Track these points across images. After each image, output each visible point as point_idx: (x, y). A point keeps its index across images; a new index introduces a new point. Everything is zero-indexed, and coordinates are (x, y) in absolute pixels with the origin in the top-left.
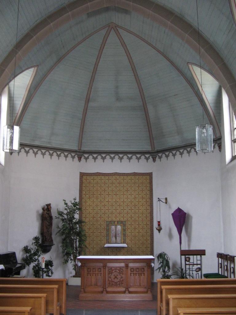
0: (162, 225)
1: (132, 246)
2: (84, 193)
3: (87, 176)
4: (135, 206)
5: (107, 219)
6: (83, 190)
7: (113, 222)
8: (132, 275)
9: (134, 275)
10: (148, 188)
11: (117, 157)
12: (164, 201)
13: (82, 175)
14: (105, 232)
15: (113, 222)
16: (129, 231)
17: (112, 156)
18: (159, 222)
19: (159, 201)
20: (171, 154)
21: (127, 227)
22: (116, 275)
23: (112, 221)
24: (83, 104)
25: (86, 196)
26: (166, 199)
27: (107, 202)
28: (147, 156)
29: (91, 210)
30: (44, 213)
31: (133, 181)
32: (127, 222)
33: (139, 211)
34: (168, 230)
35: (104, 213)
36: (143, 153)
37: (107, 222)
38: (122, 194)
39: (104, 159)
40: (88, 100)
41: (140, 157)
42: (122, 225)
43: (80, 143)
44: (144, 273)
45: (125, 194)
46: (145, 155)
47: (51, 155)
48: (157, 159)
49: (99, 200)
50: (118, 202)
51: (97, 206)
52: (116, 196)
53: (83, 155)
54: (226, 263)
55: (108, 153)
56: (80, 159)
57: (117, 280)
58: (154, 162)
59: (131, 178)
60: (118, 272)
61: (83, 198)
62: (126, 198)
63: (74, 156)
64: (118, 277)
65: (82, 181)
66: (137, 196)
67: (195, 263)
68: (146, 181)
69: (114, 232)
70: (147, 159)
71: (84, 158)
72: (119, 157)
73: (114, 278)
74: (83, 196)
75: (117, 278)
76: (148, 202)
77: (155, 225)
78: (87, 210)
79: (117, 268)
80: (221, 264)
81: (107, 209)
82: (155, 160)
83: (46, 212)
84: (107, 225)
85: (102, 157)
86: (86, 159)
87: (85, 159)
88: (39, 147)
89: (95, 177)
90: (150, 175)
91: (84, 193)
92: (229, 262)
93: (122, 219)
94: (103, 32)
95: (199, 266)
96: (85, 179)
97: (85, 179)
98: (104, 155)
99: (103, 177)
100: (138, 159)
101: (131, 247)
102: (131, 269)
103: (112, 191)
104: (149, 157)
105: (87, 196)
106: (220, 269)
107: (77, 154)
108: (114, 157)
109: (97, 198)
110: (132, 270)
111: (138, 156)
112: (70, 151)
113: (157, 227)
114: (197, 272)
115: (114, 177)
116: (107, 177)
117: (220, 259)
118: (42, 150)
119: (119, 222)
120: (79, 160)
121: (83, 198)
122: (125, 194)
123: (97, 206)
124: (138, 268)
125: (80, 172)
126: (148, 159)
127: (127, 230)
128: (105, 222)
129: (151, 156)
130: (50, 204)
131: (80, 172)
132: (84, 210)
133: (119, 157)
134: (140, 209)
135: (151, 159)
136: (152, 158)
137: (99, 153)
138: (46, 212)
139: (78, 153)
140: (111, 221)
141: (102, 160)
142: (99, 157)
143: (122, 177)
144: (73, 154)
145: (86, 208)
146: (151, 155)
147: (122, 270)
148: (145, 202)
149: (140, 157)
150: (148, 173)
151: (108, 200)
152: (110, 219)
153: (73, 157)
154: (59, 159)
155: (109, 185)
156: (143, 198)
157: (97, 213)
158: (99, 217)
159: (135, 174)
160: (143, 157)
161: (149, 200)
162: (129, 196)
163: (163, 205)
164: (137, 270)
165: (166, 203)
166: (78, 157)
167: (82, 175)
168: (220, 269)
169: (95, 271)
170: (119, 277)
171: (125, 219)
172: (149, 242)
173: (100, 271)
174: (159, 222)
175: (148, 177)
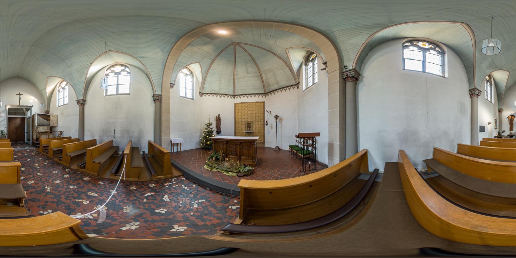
0: (268, 122)
12: (269, 112)
13: (235, 104)
16: (255, 125)
18: (267, 121)
26: (270, 112)
28: (262, 95)
35: (244, 118)
48: (267, 96)
49: (242, 113)
56: (234, 98)
74: (236, 112)
77: (265, 122)
84: (246, 123)
86: (237, 98)
89: (241, 104)
90: (264, 102)
93: (252, 121)
99: (244, 104)
103: (248, 109)
109: (241, 113)
115: (248, 104)
130: (219, 115)
135: (264, 96)
156: (260, 112)
159: (257, 102)
162: (255, 111)
165: (270, 113)
167: (235, 104)
174: (267, 121)
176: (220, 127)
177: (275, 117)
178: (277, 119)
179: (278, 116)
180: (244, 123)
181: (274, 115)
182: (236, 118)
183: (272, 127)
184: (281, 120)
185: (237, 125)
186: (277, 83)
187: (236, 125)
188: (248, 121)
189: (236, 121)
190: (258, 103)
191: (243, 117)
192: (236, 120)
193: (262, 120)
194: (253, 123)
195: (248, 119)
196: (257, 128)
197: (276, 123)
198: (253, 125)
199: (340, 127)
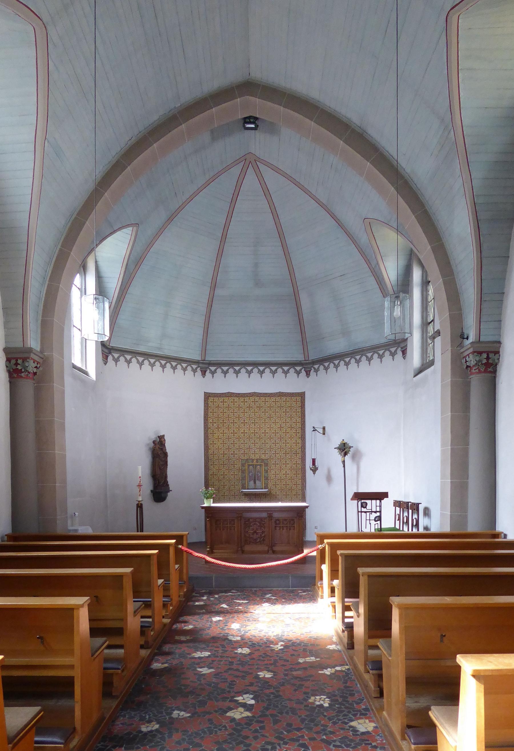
1: (276, 493)
2: (211, 421)
3: (214, 397)
4: (281, 438)
5: (243, 458)
6: (210, 417)
7: (251, 460)
8: (278, 528)
9: (280, 529)
10: (299, 414)
11: (255, 370)
12: (321, 431)
13: (207, 396)
14: (240, 474)
15: (251, 460)
16: (273, 472)
17: (249, 368)
18: (314, 461)
19: (314, 431)
20: (332, 365)
21: (270, 467)
22: (255, 529)
23: (250, 459)
24: (207, 290)
25: (213, 425)
26: (324, 428)
27: (242, 433)
28: (298, 368)
29: (221, 444)
30: (155, 447)
31: (278, 404)
32: (270, 460)
33: (286, 446)
34: (326, 472)
35: (239, 449)
36: (292, 364)
37: (243, 460)
38: (263, 423)
39: (237, 373)
40: (214, 286)
41: (288, 370)
42: (263, 464)
43: (204, 350)
44: (294, 527)
45: (267, 423)
46: (296, 368)
47: (163, 367)
50: (257, 433)
51: (229, 438)
52: (255, 425)
53: (208, 368)
54: (406, 514)
55: (244, 364)
56: (204, 373)
57: (257, 536)
58: (308, 377)
59: (276, 399)
60: (258, 524)
61: (210, 428)
62: (268, 428)
63: (196, 368)
64: (257, 532)
65: (208, 405)
66: (283, 425)
67: (374, 510)
68: (296, 404)
69: (252, 475)
70: (298, 373)
71: (210, 373)
72: (259, 370)
73: (253, 533)
74: (210, 425)
75: (257, 533)
76: (299, 433)
77: (309, 464)
78: (215, 444)
79: (257, 520)
80: (399, 515)
81: (242, 443)
82: (309, 375)
83: (158, 446)
84: (243, 465)
85: (235, 370)
86: (213, 373)
87: (211, 373)
88: (146, 355)
89: (226, 399)
90: (302, 395)
91: (211, 421)
92: (410, 511)
93: (263, 457)
94: (236, 170)
95: (378, 514)
96: (211, 402)
97: (211, 402)
98: (237, 368)
100: (286, 373)
101: (275, 494)
102: (275, 521)
103: (250, 418)
104: (301, 370)
105: (215, 425)
106: (398, 522)
107: (199, 367)
108: (252, 370)
109: (228, 428)
110: (278, 522)
111: (286, 368)
112: (190, 362)
113: (311, 467)
114: (376, 521)
115: (252, 399)
116: (242, 399)
117: (398, 509)
118: (149, 359)
119: (259, 460)
120: (202, 375)
121: (210, 428)
122: (267, 423)
123: (229, 438)
124: (286, 520)
125: (205, 392)
126: (299, 373)
127: (270, 471)
128: (239, 461)
129: (304, 369)
130: (163, 436)
131: (205, 392)
132: (211, 444)
133: (259, 370)
134: (288, 443)
135: (303, 373)
136: (305, 371)
137: (231, 364)
138: (158, 446)
139: (201, 365)
140: (247, 459)
141: (235, 375)
142: (231, 371)
143: (263, 399)
144: (194, 367)
145: (213, 442)
146: (304, 368)
147: (264, 523)
148: (294, 433)
149: (288, 370)
150: (298, 393)
151: (244, 431)
152: (246, 457)
153: (194, 371)
154: (174, 372)
155: (244, 410)
156: (291, 428)
157: (229, 449)
158: (232, 454)
159: (281, 395)
160: (292, 370)
161: (299, 430)
162: (273, 425)
163: (320, 436)
164: (285, 522)
165: (324, 434)
166: (201, 371)
167: (207, 396)
168: (398, 522)
169: (227, 524)
170: (259, 531)
171: (267, 457)
172: (300, 487)
173: (234, 524)
174: (314, 461)
175: (299, 398)
176: (166, 477)
177: (340, 449)
178: (346, 454)
179: (350, 447)
180: (238, 465)
181: (337, 443)
182: (211, 447)
183: (329, 478)
184: (357, 457)
185: (213, 470)
186: (345, 333)
187: (211, 472)
188: (252, 457)
189: (211, 457)
190: (284, 398)
191: (234, 444)
192: (210, 452)
193: (296, 453)
194: (266, 465)
195: (253, 452)
196: (281, 480)
197: (344, 466)
198: (266, 471)
199: (451, 482)
